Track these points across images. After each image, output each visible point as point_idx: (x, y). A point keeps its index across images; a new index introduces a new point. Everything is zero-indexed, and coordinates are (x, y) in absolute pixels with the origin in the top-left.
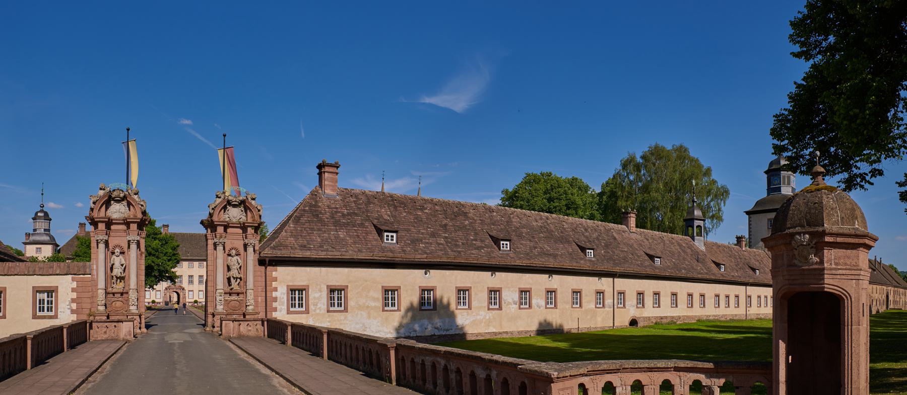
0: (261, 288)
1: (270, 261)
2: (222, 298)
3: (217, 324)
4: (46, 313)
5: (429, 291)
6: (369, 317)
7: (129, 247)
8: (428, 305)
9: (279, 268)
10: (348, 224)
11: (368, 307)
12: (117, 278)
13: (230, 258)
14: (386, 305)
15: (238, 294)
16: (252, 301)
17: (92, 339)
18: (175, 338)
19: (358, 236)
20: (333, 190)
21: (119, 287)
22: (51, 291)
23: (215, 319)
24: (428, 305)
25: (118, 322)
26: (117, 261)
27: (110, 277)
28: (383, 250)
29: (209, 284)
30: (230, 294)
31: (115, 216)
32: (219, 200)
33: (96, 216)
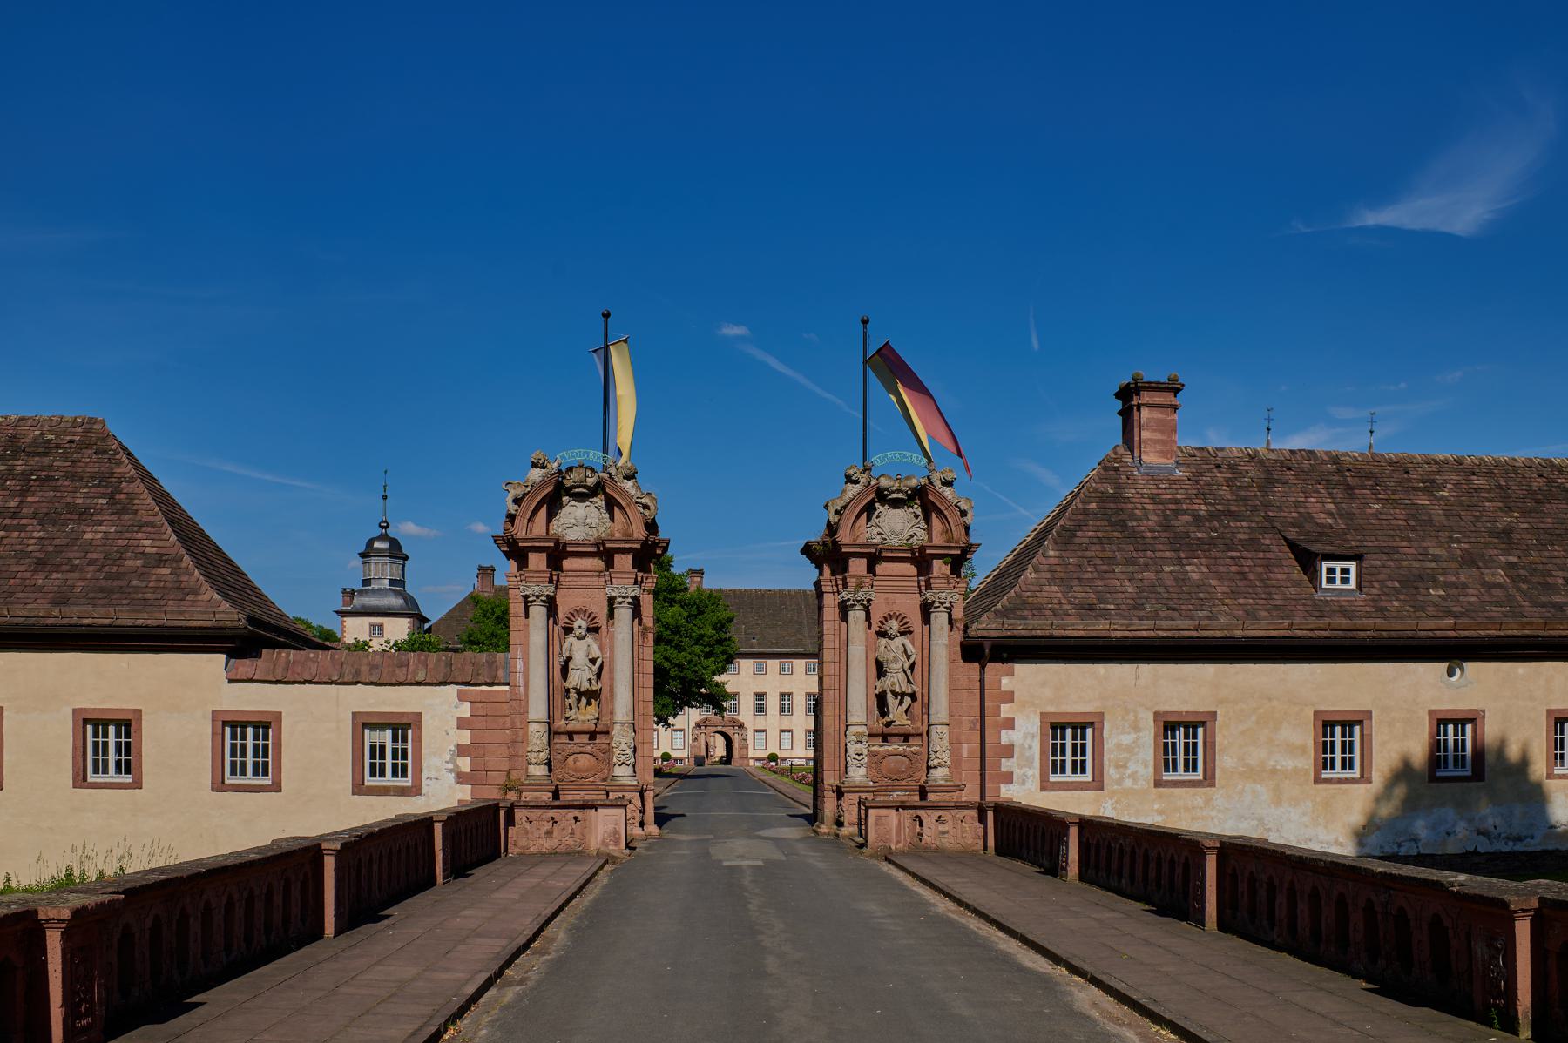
0: (969, 721)
1: (994, 648)
2: (863, 748)
3: (851, 815)
4: (388, 780)
5: (1460, 723)
6: (1277, 801)
7: (611, 615)
8: (1459, 767)
9: (1018, 667)
10: (1212, 543)
11: (1274, 772)
12: (580, 694)
13: (883, 641)
14: (1327, 764)
15: (906, 737)
16: (945, 756)
17: (513, 851)
18: (741, 852)
19: (1243, 575)
20: (1164, 454)
21: (585, 716)
22: (402, 726)
23: (845, 803)
24: (1459, 767)
25: (583, 807)
26: (580, 650)
27: (561, 692)
28: (1319, 609)
29: (828, 710)
30: (885, 738)
31: (572, 535)
32: (853, 490)
33: (522, 534)
